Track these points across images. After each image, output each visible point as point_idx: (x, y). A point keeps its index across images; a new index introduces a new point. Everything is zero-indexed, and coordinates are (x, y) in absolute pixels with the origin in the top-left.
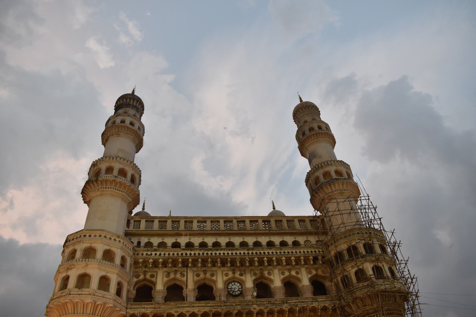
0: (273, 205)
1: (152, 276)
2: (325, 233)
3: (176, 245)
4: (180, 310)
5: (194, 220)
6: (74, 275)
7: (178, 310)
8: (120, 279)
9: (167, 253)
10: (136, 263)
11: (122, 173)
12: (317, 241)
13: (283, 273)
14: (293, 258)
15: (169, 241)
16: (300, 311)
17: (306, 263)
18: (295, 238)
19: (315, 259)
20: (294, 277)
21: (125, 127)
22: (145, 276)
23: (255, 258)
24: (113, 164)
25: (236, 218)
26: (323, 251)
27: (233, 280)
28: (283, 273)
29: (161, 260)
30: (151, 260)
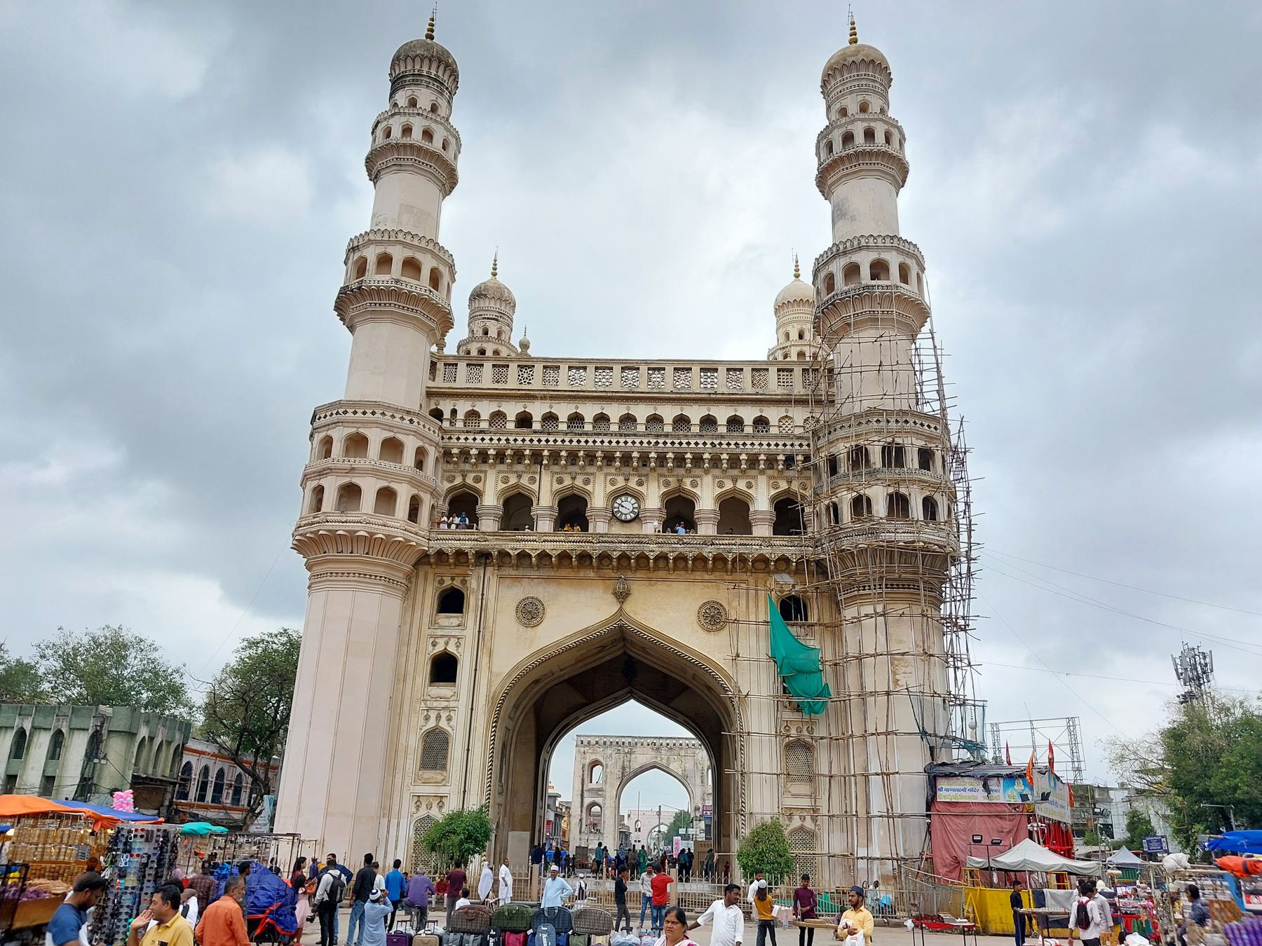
1: (477, 480)
3: (524, 421)
4: (521, 546)
6: (332, 486)
7: (516, 545)
8: (415, 492)
9: (503, 438)
10: (447, 454)
11: (412, 266)
13: (721, 485)
14: (743, 457)
16: (734, 560)
19: (790, 460)
20: (741, 492)
21: (411, 146)
24: (390, 250)
25: (646, 362)
27: (625, 492)
28: (721, 485)
30: (474, 452)
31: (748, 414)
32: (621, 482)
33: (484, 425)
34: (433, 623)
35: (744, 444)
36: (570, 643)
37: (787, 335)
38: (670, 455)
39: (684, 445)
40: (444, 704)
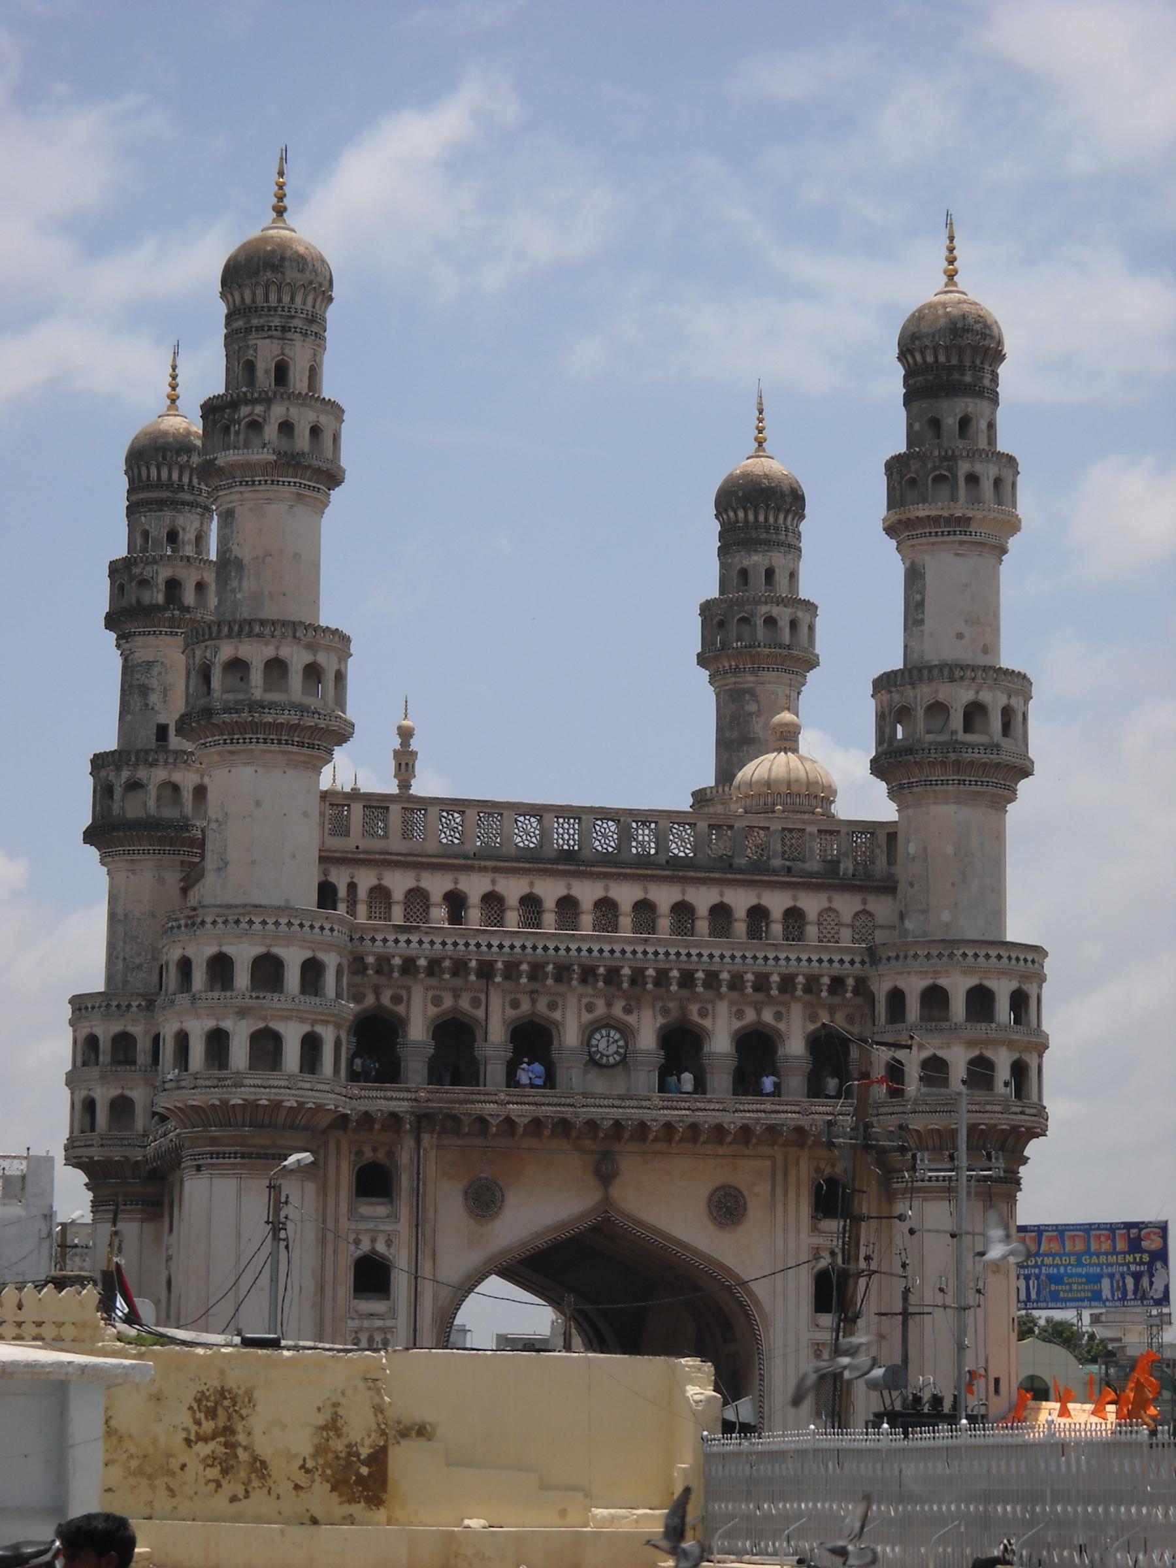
0: (761, 404)
1: (397, 999)
2: (888, 887)
3: (456, 902)
5: (506, 813)
12: (857, 914)
13: (740, 1014)
14: (775, 978)
15: (437, 885)
17: (808, 989)
18: (795, 898)
19: (837, 983)
20: (768, 1025)
22: (378, 999)
23: (671, 969)
25: (630, 812)
26: (863, 963)
28: (740, 1014)
29: (422, 962)
30: (397, 961)
31: (777, 902)
32: (601, 1009)
33: (398, 916)
34: (352, 1211)
35: (777, 959)
36: (541, 1243)
37: (744, 574)
38: (675, 973)
39: (694, 958)
40: (379, 1323)
